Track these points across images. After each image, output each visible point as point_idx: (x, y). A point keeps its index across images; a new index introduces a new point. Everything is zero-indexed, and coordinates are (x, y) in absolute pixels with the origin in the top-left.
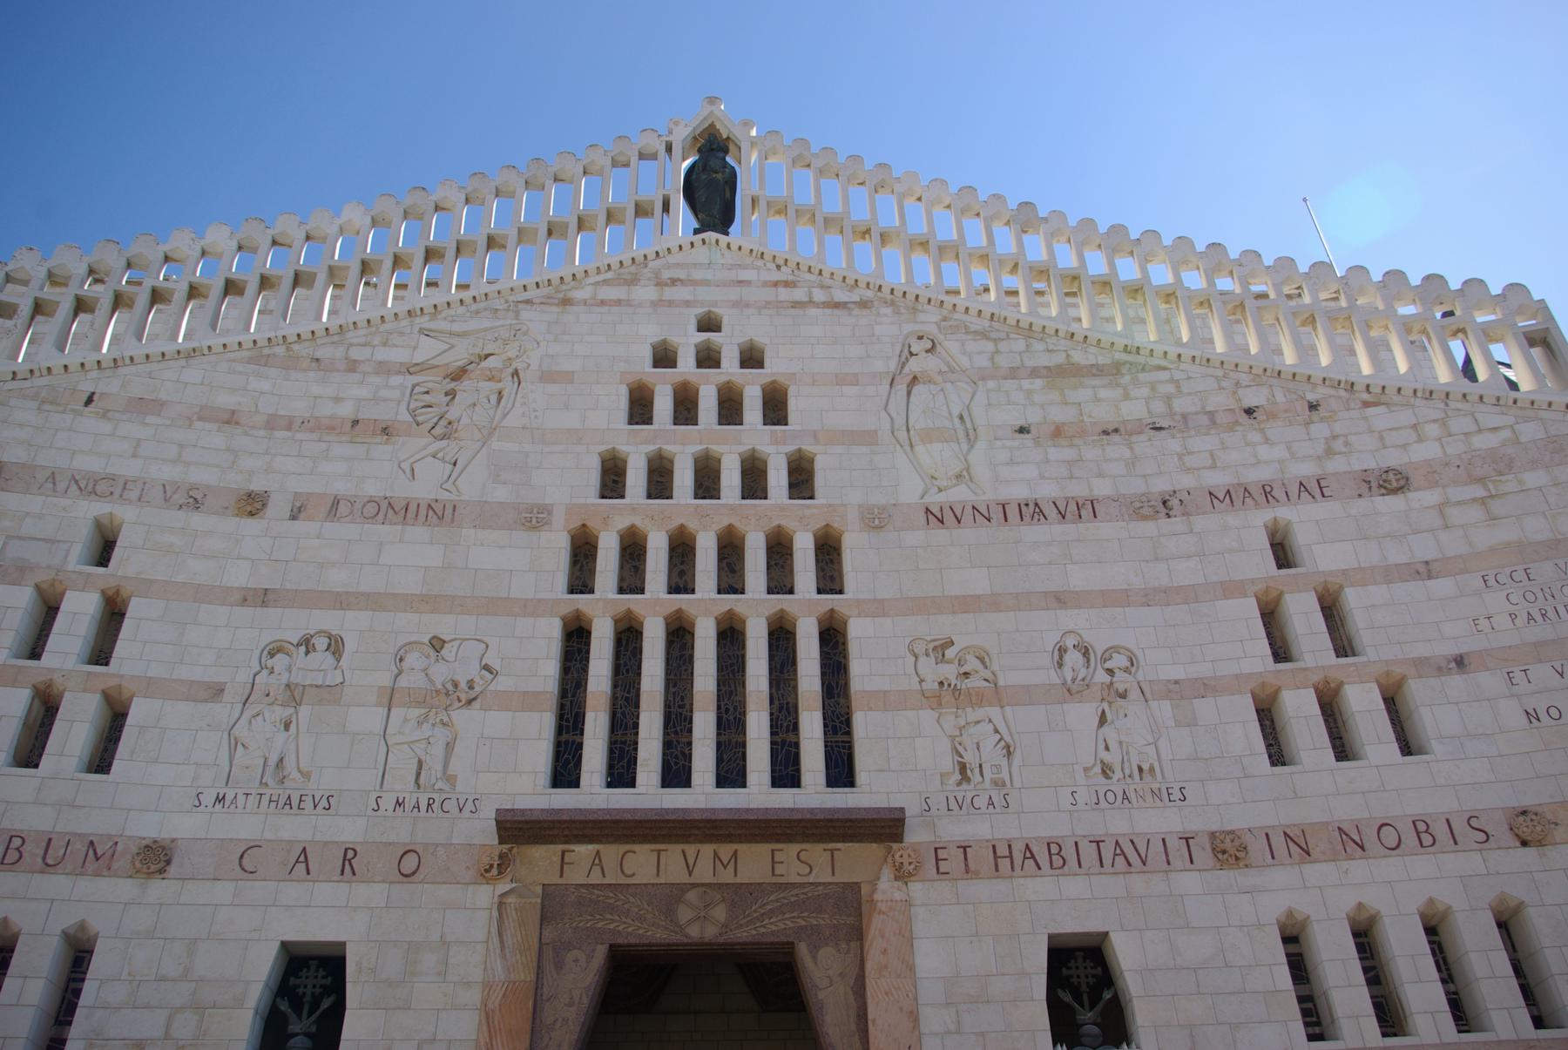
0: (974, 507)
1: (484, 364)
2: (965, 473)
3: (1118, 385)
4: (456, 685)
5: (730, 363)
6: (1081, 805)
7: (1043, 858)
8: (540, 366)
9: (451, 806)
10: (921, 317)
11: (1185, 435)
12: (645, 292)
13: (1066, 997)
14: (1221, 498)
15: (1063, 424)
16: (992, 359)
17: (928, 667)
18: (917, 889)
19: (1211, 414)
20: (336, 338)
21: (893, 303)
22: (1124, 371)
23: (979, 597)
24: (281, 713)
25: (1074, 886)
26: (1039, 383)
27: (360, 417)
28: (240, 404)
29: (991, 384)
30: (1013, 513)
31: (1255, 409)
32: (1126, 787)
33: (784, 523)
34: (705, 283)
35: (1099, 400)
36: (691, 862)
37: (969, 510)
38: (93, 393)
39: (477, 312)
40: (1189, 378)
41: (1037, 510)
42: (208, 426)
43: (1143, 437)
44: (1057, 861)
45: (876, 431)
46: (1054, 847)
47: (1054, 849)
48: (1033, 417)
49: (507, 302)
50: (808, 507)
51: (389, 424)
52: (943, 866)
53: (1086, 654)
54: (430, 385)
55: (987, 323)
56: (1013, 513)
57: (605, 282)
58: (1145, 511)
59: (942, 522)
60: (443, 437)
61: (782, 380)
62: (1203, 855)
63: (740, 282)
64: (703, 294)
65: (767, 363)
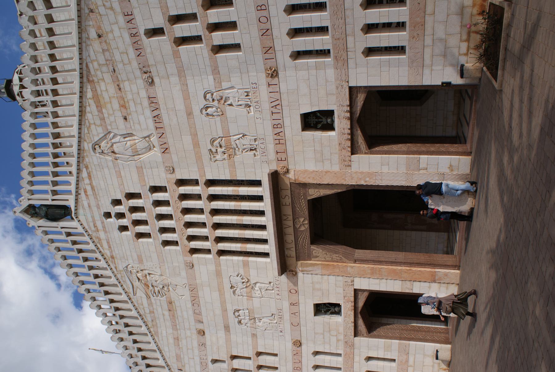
0: (160, 138)
1: (141, 278)
2: (146, 139)
3: (98, 82)
4: (243, 282)
6: (261, 116)
7: (279, 130)
8: (138, 264)
9: (277, 283)
11: (115, 61)
12: (102, 235)
13: (319, 126)
14: (140, 53)
17: (219, 157)
18: (290, 167)
20: (144, 317)
23: (193, 140)
24: (257, 321)
25: (287, 122)
26: (104, 111)
27: (167, 309)
28: (172, 337)
29: (109, 128)
30: (158, 125)
31: (98, 34)
32: (254, 101)
33: (177, 197)
34: (93, 217)
36: (288, 226)
39: (124, 281)
40: (89, 56)
41: (156, 117)
43: (119, 76)
44: (279, 126)
46: (275, 126)
47: (275, 126)
48: (119, 114)
49: (118, 274)
50: (170, 189)
51: (168, 302)
52: (283, 159)
53: (208, 107)
54: (152, 292)
56: (158, 125)
57: (102, 246)
58: (150, 81)
60: (168, 288)
61: (124, 195)
62: (275, 81)
63: (89, 206)
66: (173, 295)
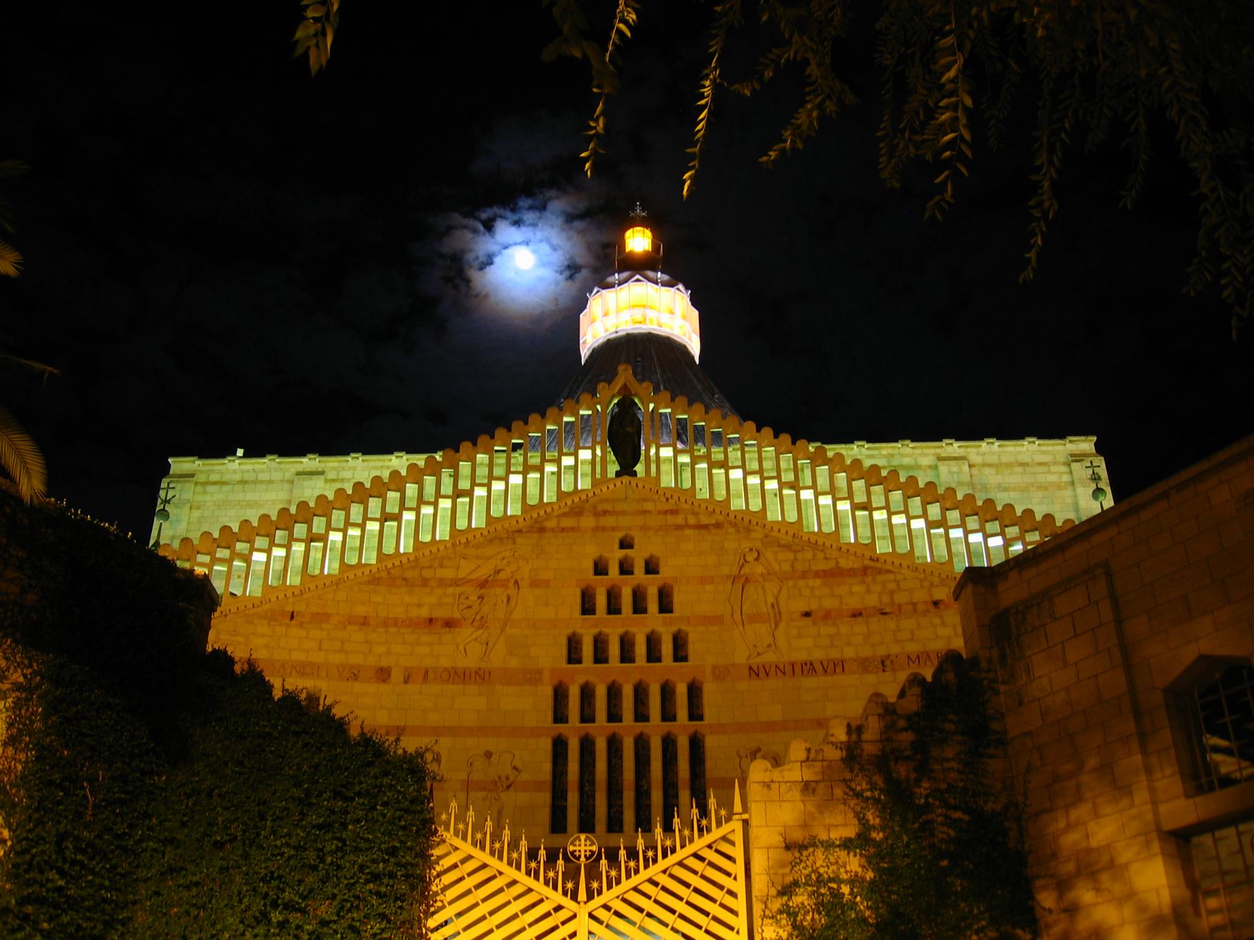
0: (776, 666)
4: (500, 778)
5: (639, 568)
8: (530, 577)
10: (753, 535)
12: (588, 522)
15: (831, 610)
16: (792, 566)
19: (915, 605)
21: (734, 525)
22: (869, 571)
26: (819, 581)
29: (791, 583)
30: (798, 669)
34: (623, 513)
35: (851, 593)
37: (773, 668)
38: (293, 613)
39: (491, 541)
40: (905, 579)
42: (355, 628)
45: (723, 616)
48: (814, 606)
55: (790, 539)
56: (798, 669)
59: (758, 675)
63: (645, 512)
64: (624, 521)
65: (662, 569)
66: (465, 634)
